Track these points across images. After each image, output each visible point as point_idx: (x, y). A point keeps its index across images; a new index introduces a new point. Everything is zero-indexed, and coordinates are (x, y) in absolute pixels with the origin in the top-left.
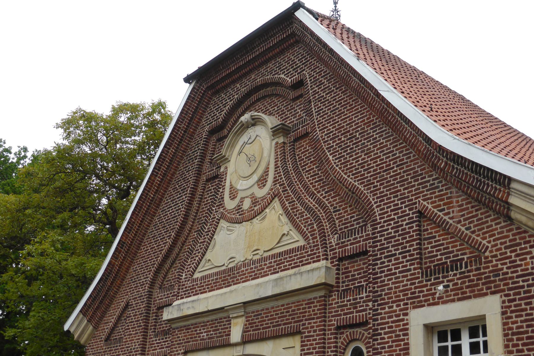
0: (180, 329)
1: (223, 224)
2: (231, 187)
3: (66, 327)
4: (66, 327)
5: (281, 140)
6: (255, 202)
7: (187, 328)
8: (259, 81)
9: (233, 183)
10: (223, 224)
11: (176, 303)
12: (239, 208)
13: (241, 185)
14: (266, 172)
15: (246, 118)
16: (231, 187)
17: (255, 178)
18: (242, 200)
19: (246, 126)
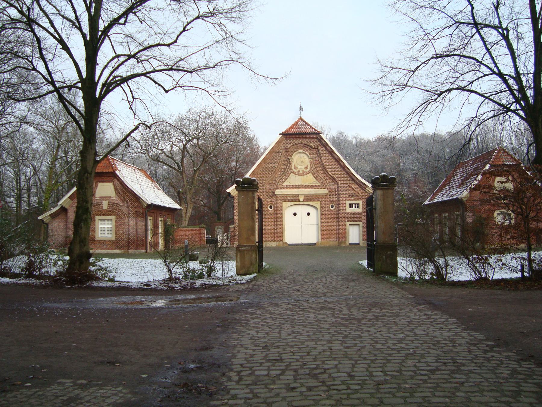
0: (280, 196)
1: (292, 174)
2: (295, 166)
3: (228, 191)
4: (228, 191)
5: (312, 160)
6: (304, 172)
7: (283, 196)
8: (303, 142)
9: (296, 165)
10: (292, 174)
11: (277, 190)
12: (298, 172)
13: (298, 167)
14: (307, 166)
15: (300, 151)
16: (295, 166)
17: (304, 167)
18: (299, 171)
19: (299, 153)
